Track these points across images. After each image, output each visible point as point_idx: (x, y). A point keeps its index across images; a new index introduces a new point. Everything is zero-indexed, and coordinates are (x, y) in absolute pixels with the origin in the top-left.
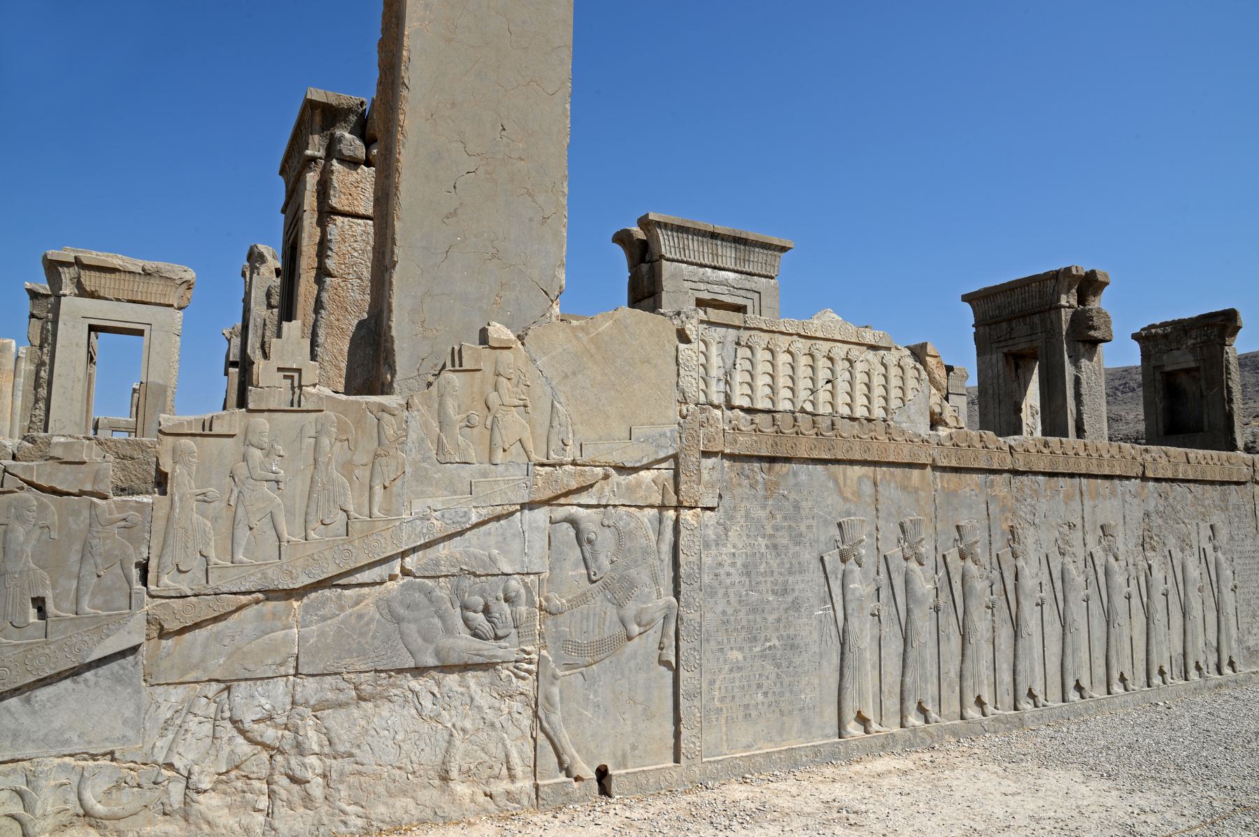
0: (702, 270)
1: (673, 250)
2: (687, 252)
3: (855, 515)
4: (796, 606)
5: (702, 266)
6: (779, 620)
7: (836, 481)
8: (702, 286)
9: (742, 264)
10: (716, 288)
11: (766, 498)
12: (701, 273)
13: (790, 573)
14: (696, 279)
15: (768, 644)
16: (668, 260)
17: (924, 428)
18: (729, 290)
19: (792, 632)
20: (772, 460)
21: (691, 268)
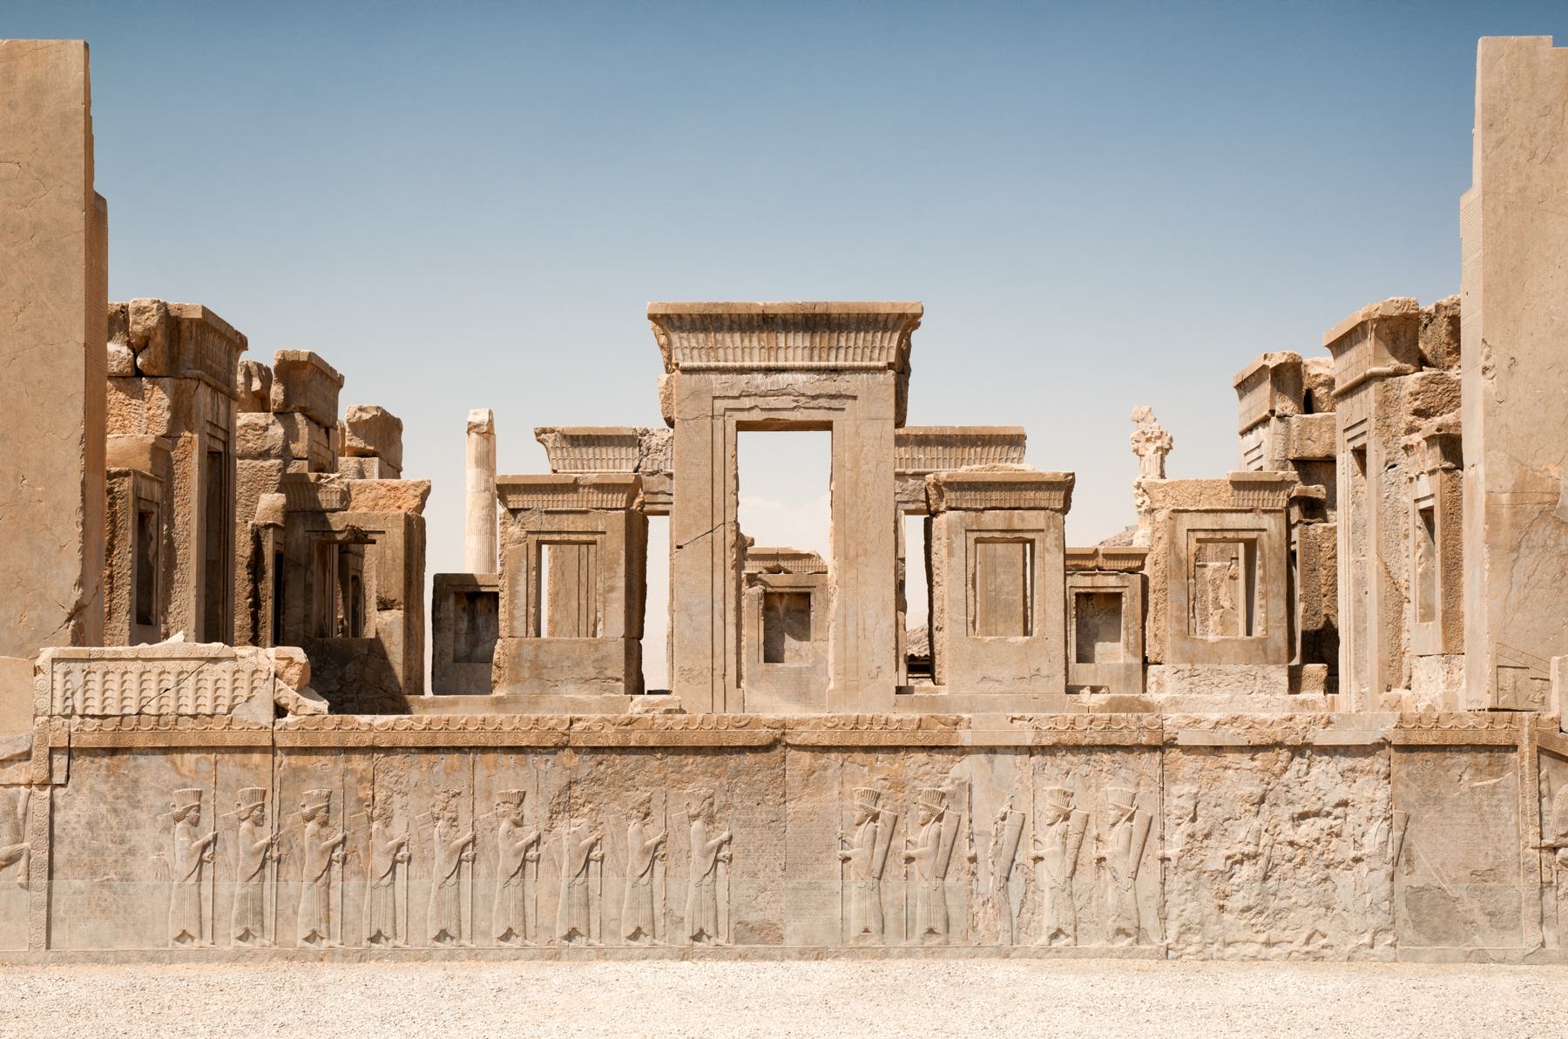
1: (695, 352)
2: (721, 352)
3: (191, 786)
4: (132, 852)
5: (742, 371)
6: (116, 862)
7: (174, 763)
8: (747, 402)
9: (824, 355)
10: (773, 402)
11: (108, 776)
12: (743, 383)
13: (127, 829)
15: (106, 877)
16: (685, 371)
17: (266, 716)
18: (794, 401)
19: (128, 870)
20: (113, 751)
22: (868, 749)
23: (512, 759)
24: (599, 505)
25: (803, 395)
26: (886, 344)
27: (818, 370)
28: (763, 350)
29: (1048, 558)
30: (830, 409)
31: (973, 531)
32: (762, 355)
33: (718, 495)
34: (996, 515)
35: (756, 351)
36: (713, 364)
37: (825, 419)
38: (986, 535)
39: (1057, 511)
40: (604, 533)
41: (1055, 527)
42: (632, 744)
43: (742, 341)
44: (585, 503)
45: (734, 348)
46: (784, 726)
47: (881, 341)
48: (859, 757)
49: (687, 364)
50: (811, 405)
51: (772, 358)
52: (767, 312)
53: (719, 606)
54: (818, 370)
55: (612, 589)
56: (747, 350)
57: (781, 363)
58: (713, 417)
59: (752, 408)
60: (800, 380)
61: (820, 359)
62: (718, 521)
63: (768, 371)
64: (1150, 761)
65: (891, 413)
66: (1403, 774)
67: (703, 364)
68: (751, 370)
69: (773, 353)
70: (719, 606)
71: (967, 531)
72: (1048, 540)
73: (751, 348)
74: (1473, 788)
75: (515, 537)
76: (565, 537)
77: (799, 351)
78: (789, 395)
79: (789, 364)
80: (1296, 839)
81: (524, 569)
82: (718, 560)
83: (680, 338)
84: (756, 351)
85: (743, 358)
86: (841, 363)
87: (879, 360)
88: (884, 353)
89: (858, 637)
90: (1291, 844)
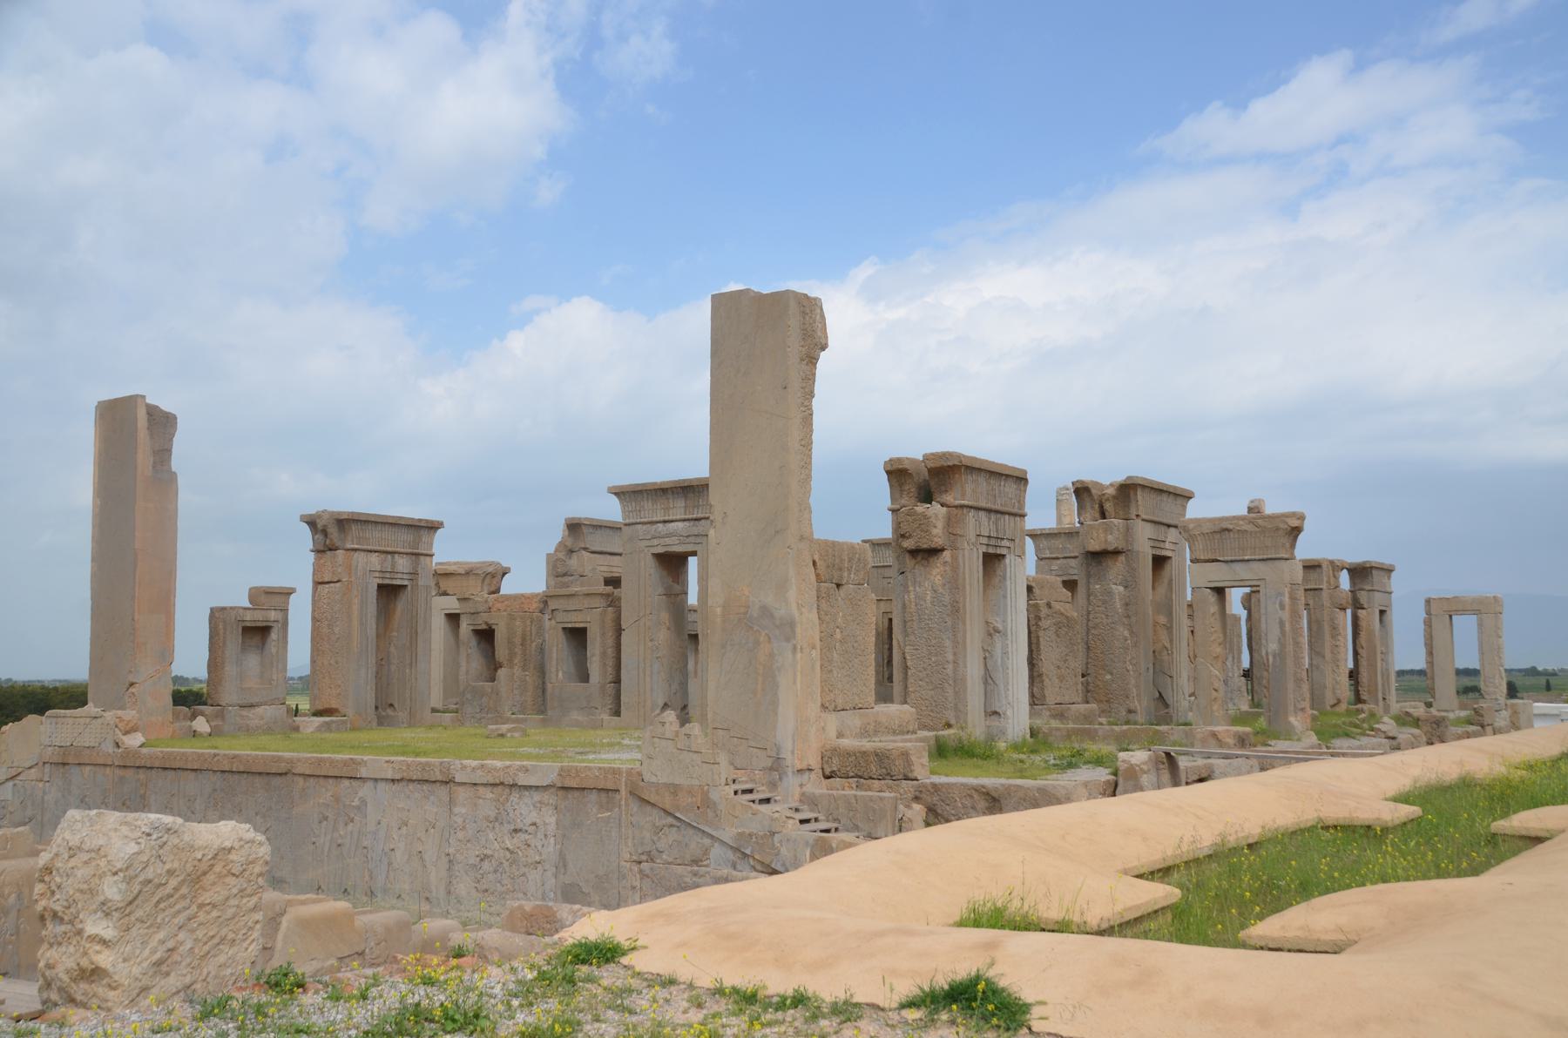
2: (642, 513)
8: (655, 542)
21: (645, 527)
22: (326, 777)
23: (192, 775)
27: (688, 520)
36: (638, 521)
37: (693, 550)
42: (234, 770)
43: (653, 505)
46: (292, 762)
48: (322, 781)
54: (688, 520)
55: (593, 655)
57: (671, 518)
61: (702, 513)
63: (665, 522)
64: (442, 792)
66: (563, 807)
74: (598, 819)
79: (674, 518)
80: (509, 846)
86: (700, 515)
90: (507, 849)
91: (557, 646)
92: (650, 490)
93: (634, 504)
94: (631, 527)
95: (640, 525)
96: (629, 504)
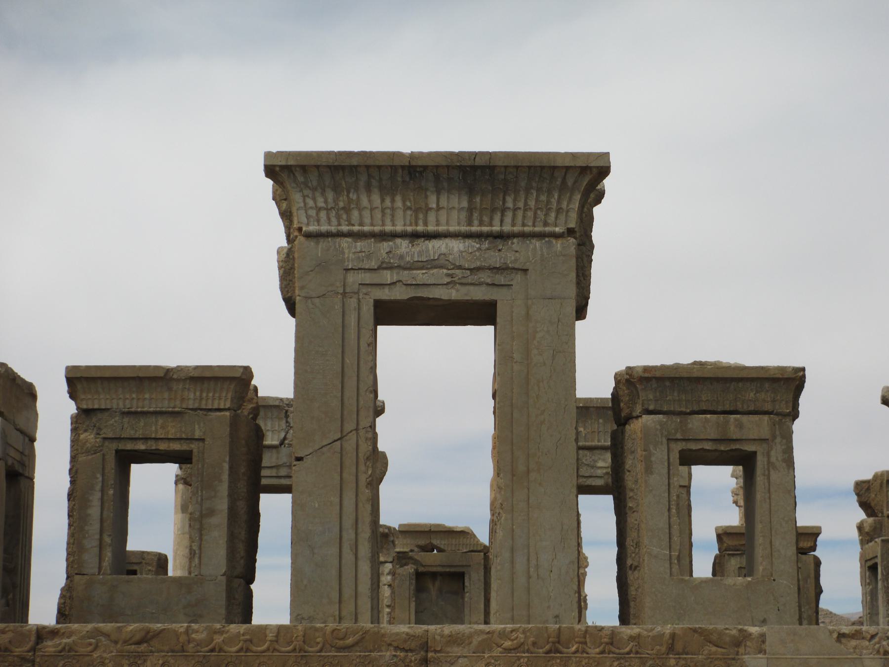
0: (385, 246)
1: (323, 214)
2: (355, 214)
5: (384, 236)
8: (388, 276)
10: (420, 276)
14: (373, 264)
18: (448, 275)
24: (196, 406)
25: (460, 267)
26: (564, 205)
28: (409, 212)
29: (774, 476)
30: (493, 285)
31: (677, 440)
32: (408, 218)
33: (350, 392)
34: (707, 420)
35: (399, 214)
36: (345, 228)
37: (487, 297)
38: (694, 446)
39: (785, 415)
40: (203, 440)
41: (783, 437)
43: (383, 201)
44: (178, 403)
45: (372, 210)
47: (559, 202)
49: (313, 228)
50: (469, 280)
51: (421, 222)
52: (413, 163)
53: (349, 535)
55: (211, 512)
56: (388, 211)
57: (431, 228)
58: (344, 294)
59: (394, 283)
60: (456, 249)
62: (349, 426)
63: (415, 236)
65: (572, 291)
67: (333, 229)
68: (394, 236)
69: (421, 216)
70: (349, 535)
71: (668, 440)
72: (773, 453)
73: (393, 209)
75: (88, 445)
76: (152, 445)
77: (455, 214)
78: (441, 267)
79: (442, 228)
81: (98, 487)
82: (349, 477)
83: (304, 197)
84: (399, 214)
85: (383, 221)
86: (507, 228)
87: (556, 226)
88: (562, 217)
89: (529, 577)
91: (102, 491)
92: (379, 167)
93: (330, 195)
94: (323, 244)
95: (349, 240)
96: (318, 194)
